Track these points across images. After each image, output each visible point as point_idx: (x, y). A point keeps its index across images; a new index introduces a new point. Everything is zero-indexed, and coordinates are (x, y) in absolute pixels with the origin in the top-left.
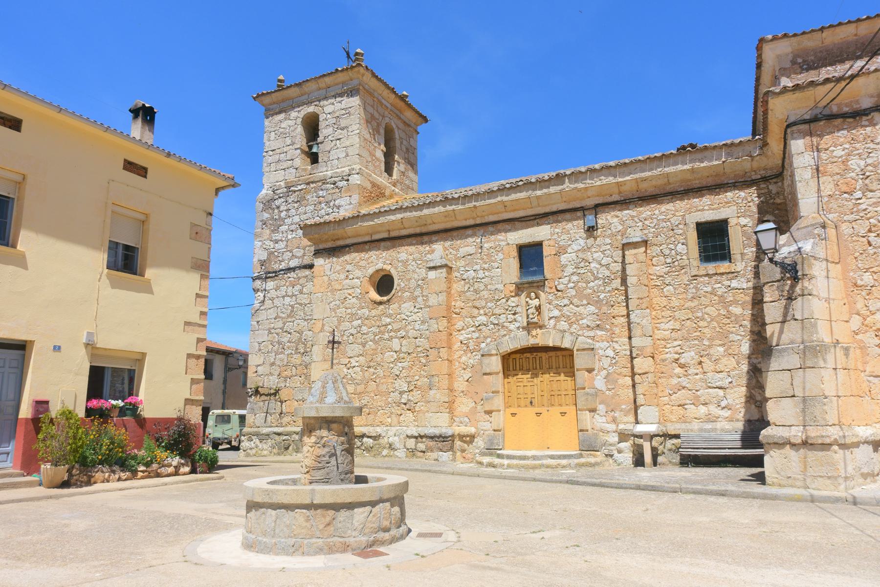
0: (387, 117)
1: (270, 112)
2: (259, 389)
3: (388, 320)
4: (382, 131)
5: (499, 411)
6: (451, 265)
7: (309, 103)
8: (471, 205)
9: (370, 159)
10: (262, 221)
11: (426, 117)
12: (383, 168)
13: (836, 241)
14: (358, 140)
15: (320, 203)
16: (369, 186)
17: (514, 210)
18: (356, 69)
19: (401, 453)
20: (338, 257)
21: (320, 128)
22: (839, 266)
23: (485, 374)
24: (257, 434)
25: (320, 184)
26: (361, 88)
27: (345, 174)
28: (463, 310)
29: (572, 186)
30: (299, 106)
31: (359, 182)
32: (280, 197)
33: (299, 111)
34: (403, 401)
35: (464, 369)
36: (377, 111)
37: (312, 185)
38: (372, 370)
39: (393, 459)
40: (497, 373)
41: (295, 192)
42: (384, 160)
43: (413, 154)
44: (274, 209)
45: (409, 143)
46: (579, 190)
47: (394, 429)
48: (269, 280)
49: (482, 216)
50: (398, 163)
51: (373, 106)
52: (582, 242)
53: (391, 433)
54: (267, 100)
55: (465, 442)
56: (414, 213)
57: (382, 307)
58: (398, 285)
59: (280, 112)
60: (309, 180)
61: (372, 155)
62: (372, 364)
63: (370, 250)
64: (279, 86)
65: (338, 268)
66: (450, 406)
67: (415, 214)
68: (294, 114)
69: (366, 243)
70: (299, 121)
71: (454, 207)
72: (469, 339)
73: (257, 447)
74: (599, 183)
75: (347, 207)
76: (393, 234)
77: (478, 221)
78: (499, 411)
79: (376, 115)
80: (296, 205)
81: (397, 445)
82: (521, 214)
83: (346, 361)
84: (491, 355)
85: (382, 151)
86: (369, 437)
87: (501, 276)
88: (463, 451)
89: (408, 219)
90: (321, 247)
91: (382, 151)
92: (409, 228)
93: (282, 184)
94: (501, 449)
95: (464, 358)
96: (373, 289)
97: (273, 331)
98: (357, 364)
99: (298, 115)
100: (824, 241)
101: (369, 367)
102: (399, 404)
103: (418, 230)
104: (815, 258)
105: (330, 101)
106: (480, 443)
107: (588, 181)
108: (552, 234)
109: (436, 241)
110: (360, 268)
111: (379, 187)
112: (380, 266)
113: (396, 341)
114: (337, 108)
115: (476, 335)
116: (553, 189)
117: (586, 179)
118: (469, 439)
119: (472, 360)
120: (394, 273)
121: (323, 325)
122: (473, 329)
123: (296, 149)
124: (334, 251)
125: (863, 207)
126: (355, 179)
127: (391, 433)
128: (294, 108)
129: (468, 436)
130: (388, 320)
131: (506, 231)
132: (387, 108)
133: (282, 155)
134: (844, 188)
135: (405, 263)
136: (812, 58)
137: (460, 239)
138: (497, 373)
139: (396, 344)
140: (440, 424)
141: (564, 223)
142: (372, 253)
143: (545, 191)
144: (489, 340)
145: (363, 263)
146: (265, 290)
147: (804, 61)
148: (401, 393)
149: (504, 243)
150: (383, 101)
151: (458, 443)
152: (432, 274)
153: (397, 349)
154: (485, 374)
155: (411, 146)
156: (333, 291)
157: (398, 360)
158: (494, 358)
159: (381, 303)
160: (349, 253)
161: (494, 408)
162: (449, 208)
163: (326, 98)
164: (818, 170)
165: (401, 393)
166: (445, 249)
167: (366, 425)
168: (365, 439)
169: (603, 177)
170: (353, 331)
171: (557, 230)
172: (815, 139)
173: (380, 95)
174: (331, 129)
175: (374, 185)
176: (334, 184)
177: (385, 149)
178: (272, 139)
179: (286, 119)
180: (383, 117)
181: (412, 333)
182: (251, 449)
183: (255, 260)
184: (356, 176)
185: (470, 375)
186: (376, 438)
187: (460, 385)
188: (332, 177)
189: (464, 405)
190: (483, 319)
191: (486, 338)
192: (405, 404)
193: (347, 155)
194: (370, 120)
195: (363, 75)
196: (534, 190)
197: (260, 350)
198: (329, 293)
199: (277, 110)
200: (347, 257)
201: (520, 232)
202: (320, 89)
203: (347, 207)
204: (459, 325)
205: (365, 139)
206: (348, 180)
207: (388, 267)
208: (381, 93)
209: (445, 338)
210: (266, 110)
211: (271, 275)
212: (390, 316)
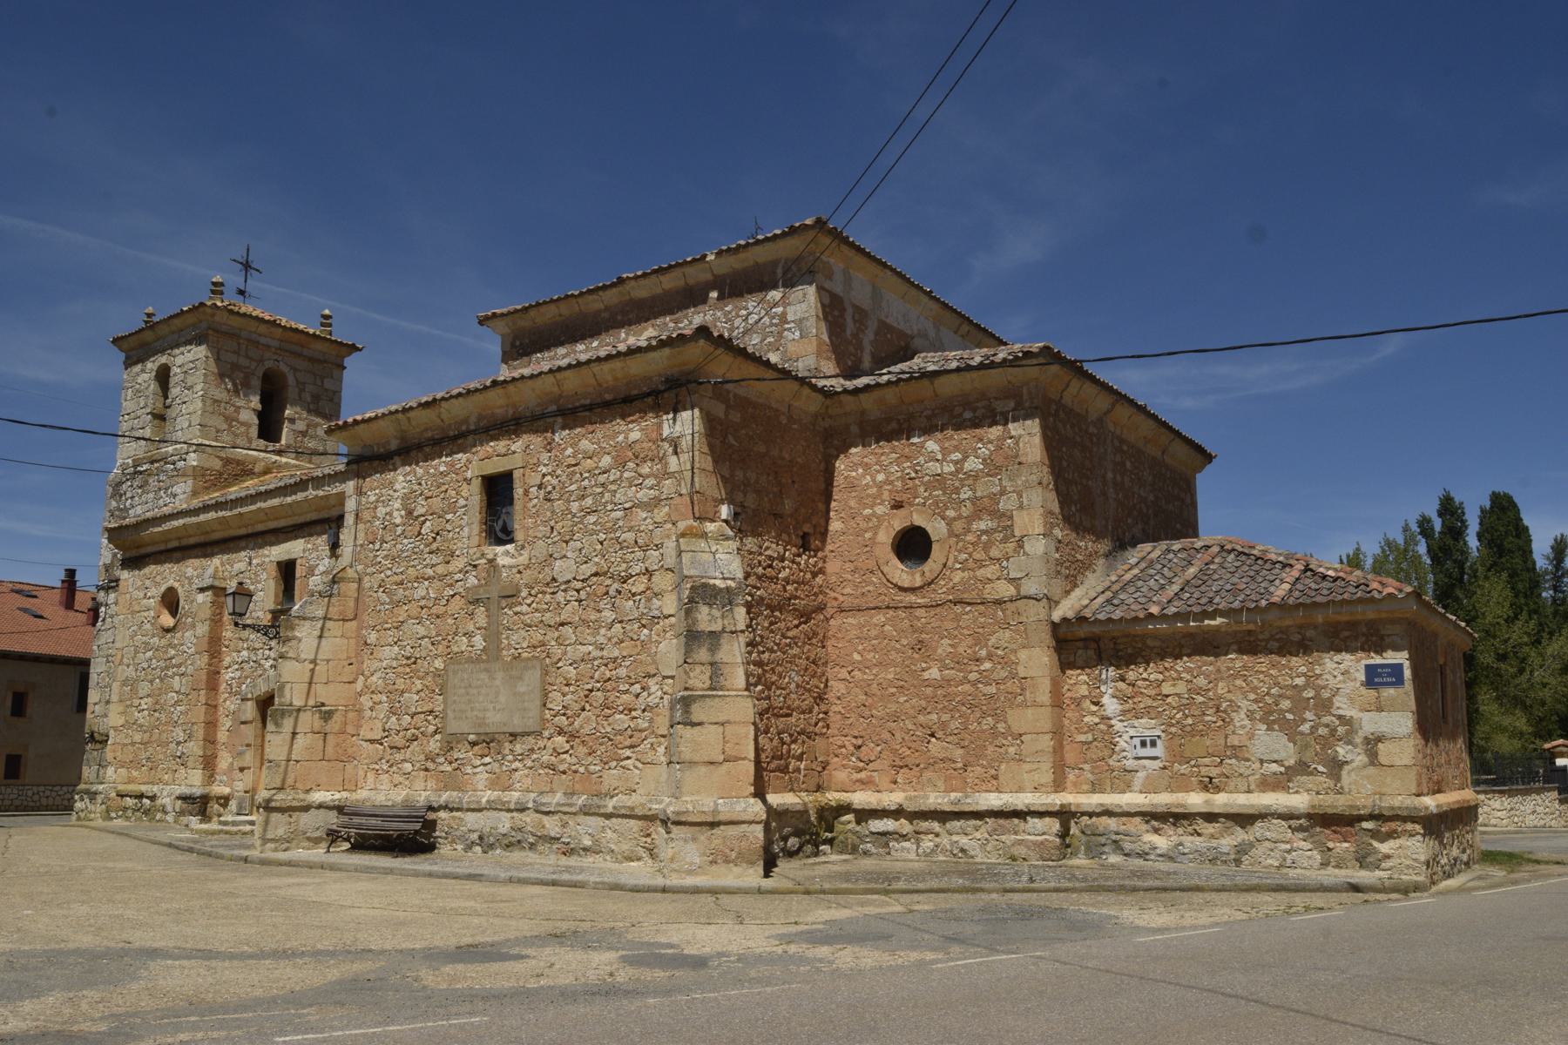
0: (269, 359)
1: (128, 364)
2: (95, 735)
3: (173, 652)
4: (256, 383)
5: (249, 768)
6: (223, 585)
7: (162, 351)
8: (235, 512)
9: (225, 426)
10: (110, 511)
11: (354, 345)
12: (254, 431)
13: (356, 595)
14: (200, 404)
15: (160, 489)
16: (217, 464)
17: (277, 519)
18: (201, 309)
19: (170, 818)
20: (140, 570)
21: (171, 385)
22: (354, 623)
23: (243, 723)
24: (87, 792)
25: (162, 463)
26: (210, 332)
27: (183, 451)
28: (232, 643)
29: (314, 493)
30: (154, 355)
31: (195, 463)
32: (128, 480)
33: (154, 362)
34: (178, 754)
35: (227, 716)
36: (247, 356)
37: (156, 465)
38: (157, 714)
39: (164, 824)
40: (251, 722)
41: (141, 473)
42: (257, 422)
43: (331, 400)
44: (121, 496)
45: (322, 386)
46: (322, 497)
47: (169, 787)
48: (110, 591)
49: (252, 525)
50: (292, 421)
51: (237, 353)
52: (327, 561)
53: (165, 793)
54: (125, 345)
55: (221, 805)
56: (193, 519)
57: (169, 635)
58: (183, 608)
59: (136, 363)
60: (154, 458)
61: (229, 420)
62: (158, 707)
63: (165, 562)
64: (146, 322)
65: (140, 583)
66: (209, 763)
67: (194, 520)
68: (149, 365)
69: (161, 552)
70: (154, 374)
71: (224, 512)
72: (233, 679)
73: (87, 807)
74: (334, 491)
75: (182, 497)
76: (185, 542)
77: (250, 531)
78: (249, 768)
79: (243, 362)
80: (140, 491)
81: (169, 808)
82: (282, 523)
83: (136, 702)
84: (248, 700)
85: (254, 410)
86: (147, 797)
87: (263, 601)
88: (220, 816)
89: (191, 525)
90: (128, 555)
91: (254, 410)
92: (194, 536)
93: (130, 461)
94: (247, 815)
95: (228, 702)
96: (166, 612)
97: (110, 659)
98: (146, 707)
99: (152, 365)
100: (326, 599)
101: (155, 711)
102: (175, 757)
103: (202, 539)
104: (304, 619)
105: (182, 349)
106: (233, 805)
107: (326, 488)
108: (304, 551)
109: (217, 554)
110: (157, 584)
111: (238, 462)
112: (171, 583)
113: (177, 678)
114: (187, 360)
115: (238, 674)
116: (300, 496)
117: (323, 486)
118: (224, 801)
119: (231, 704)
120: (180, 590)
121: (123, 655)
122: (236, 666)
123: (148, 414)
124: (134, 561)
125: (379, 559)
126: (193, 460)
127: (165, 793)
128: (150, 357)
129: (221, 798)
130: (173, 652)
131: (272, 544)
132: (268, 347)
133: (136, 421)
134: (371, 539)
135: (190, 579)
136: (527, 341)
137: (236, 552)
138: (251, 722)
139: (176, 680)
140: (193, 781)
141: (315, 537)
142: (167, 565)
143: (294, 497)
144: (249, 680)
145: (158, 579)
146: (107, 605)
147: (521, 344)
148: (178, 743)
149: (267, 560)
150: (263, 340)
151: (215, 807)
152: (201, 598)
153: (177, 689)
154: (243, 723)
155: (326, 390)
156: (133, 613)
157: (177, 703)
158: (249, 703)
159: (168, 630)
160: (148, 564)
161: (245, 765)
162: (221, 514)
163: (178, 346)
164: (357, 515)
165: (178, 743)
166: (223, 564)
167: (148, 783)
168: (145, 800)
169: (337, 484)
170: (145, 665)
171: (309, 546)
172: (361, 481)
173: (255, 332)
174: (179, 389)
175: (227, 461)
176: (174, 464)
177: (259, 407)
178: (129, 398)
179: (143, 371)
180: (261, 361)
181: (190, 670)
182: (82, 811)
183: (101, 563)
184: (192, 455)
185: (230, 723)
186: (153, 798)
187: (222, 736)
188: (172, 455)
189: (224, 761)
190: (245, 653)
191: (246, 678)
192: (180, 757)
193: (190, 426)
194: (229, 371)
195: (213, 315)
196: (285, 496)
197: (98, 683)
198: (129, 616)
199: (135, 359)
200: (147, 570)
201: (282, 545)
202: (173, 332)
203: (182, 497)
204: (227, 660)
205: (216, 401)
206: (185, 460)
207: (176, 585)
208: (253, 330)
209: (204, 677)
210: (126, 358)
211: (113, 584)
212: (174, 647)
